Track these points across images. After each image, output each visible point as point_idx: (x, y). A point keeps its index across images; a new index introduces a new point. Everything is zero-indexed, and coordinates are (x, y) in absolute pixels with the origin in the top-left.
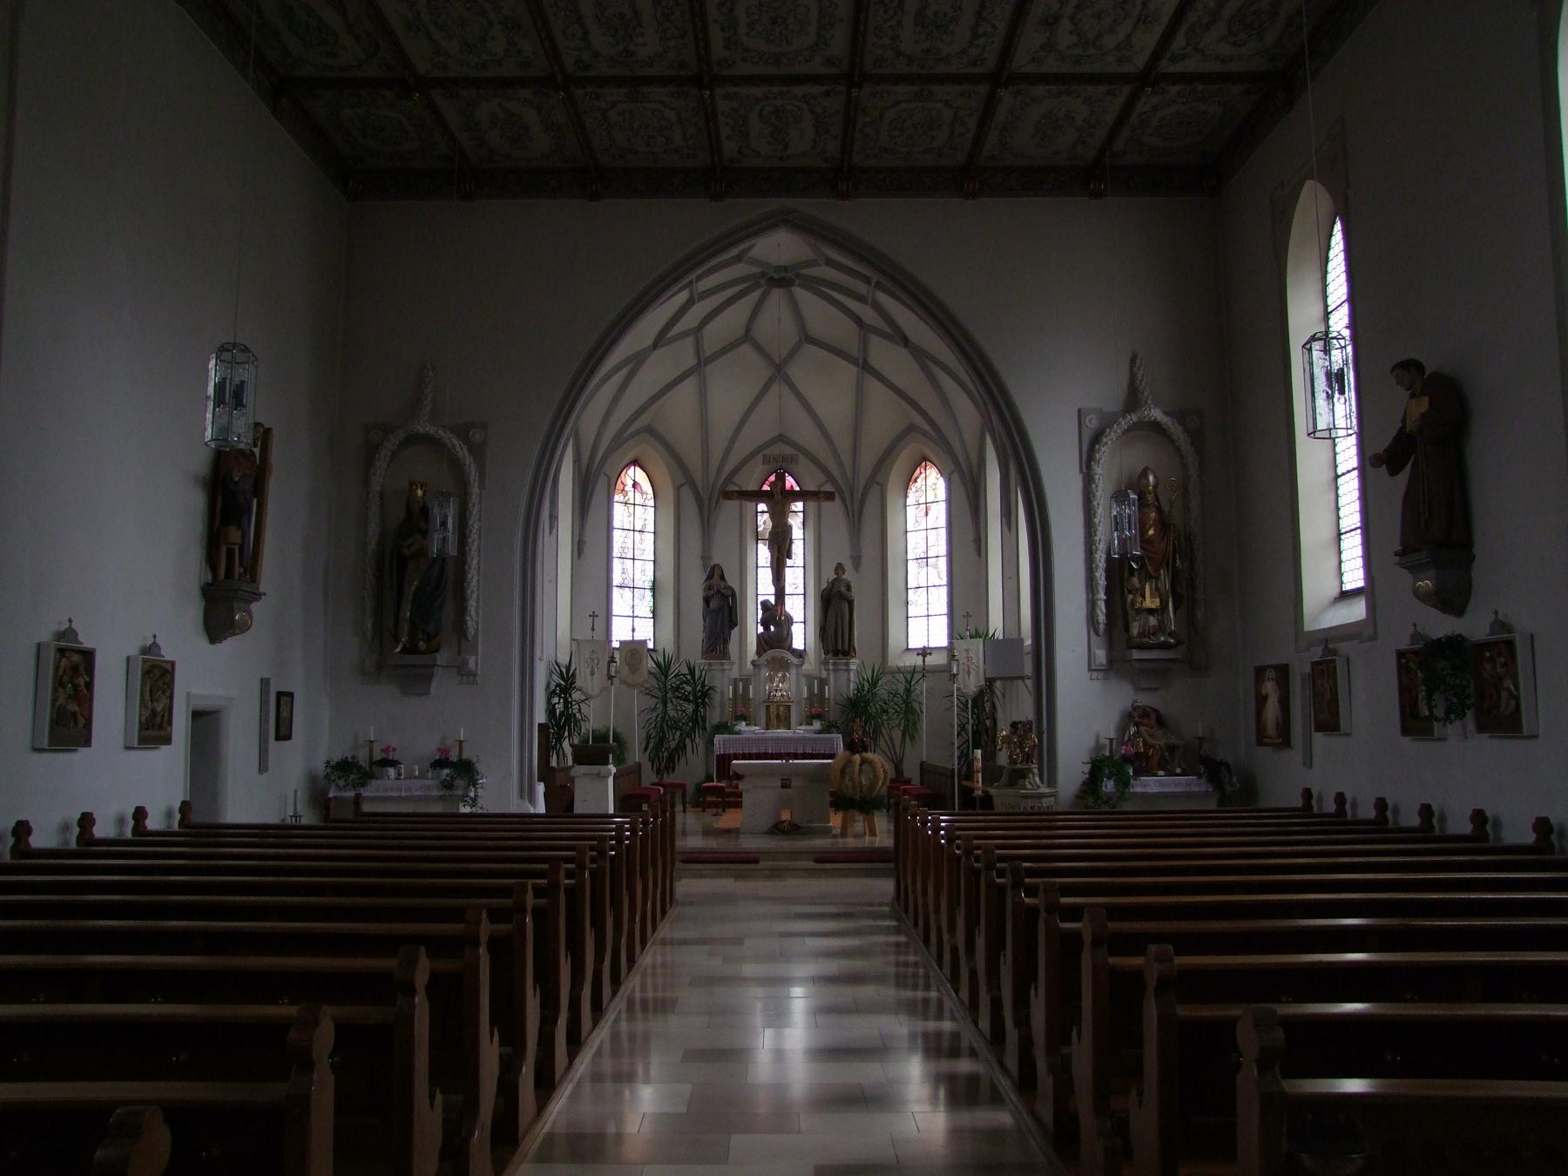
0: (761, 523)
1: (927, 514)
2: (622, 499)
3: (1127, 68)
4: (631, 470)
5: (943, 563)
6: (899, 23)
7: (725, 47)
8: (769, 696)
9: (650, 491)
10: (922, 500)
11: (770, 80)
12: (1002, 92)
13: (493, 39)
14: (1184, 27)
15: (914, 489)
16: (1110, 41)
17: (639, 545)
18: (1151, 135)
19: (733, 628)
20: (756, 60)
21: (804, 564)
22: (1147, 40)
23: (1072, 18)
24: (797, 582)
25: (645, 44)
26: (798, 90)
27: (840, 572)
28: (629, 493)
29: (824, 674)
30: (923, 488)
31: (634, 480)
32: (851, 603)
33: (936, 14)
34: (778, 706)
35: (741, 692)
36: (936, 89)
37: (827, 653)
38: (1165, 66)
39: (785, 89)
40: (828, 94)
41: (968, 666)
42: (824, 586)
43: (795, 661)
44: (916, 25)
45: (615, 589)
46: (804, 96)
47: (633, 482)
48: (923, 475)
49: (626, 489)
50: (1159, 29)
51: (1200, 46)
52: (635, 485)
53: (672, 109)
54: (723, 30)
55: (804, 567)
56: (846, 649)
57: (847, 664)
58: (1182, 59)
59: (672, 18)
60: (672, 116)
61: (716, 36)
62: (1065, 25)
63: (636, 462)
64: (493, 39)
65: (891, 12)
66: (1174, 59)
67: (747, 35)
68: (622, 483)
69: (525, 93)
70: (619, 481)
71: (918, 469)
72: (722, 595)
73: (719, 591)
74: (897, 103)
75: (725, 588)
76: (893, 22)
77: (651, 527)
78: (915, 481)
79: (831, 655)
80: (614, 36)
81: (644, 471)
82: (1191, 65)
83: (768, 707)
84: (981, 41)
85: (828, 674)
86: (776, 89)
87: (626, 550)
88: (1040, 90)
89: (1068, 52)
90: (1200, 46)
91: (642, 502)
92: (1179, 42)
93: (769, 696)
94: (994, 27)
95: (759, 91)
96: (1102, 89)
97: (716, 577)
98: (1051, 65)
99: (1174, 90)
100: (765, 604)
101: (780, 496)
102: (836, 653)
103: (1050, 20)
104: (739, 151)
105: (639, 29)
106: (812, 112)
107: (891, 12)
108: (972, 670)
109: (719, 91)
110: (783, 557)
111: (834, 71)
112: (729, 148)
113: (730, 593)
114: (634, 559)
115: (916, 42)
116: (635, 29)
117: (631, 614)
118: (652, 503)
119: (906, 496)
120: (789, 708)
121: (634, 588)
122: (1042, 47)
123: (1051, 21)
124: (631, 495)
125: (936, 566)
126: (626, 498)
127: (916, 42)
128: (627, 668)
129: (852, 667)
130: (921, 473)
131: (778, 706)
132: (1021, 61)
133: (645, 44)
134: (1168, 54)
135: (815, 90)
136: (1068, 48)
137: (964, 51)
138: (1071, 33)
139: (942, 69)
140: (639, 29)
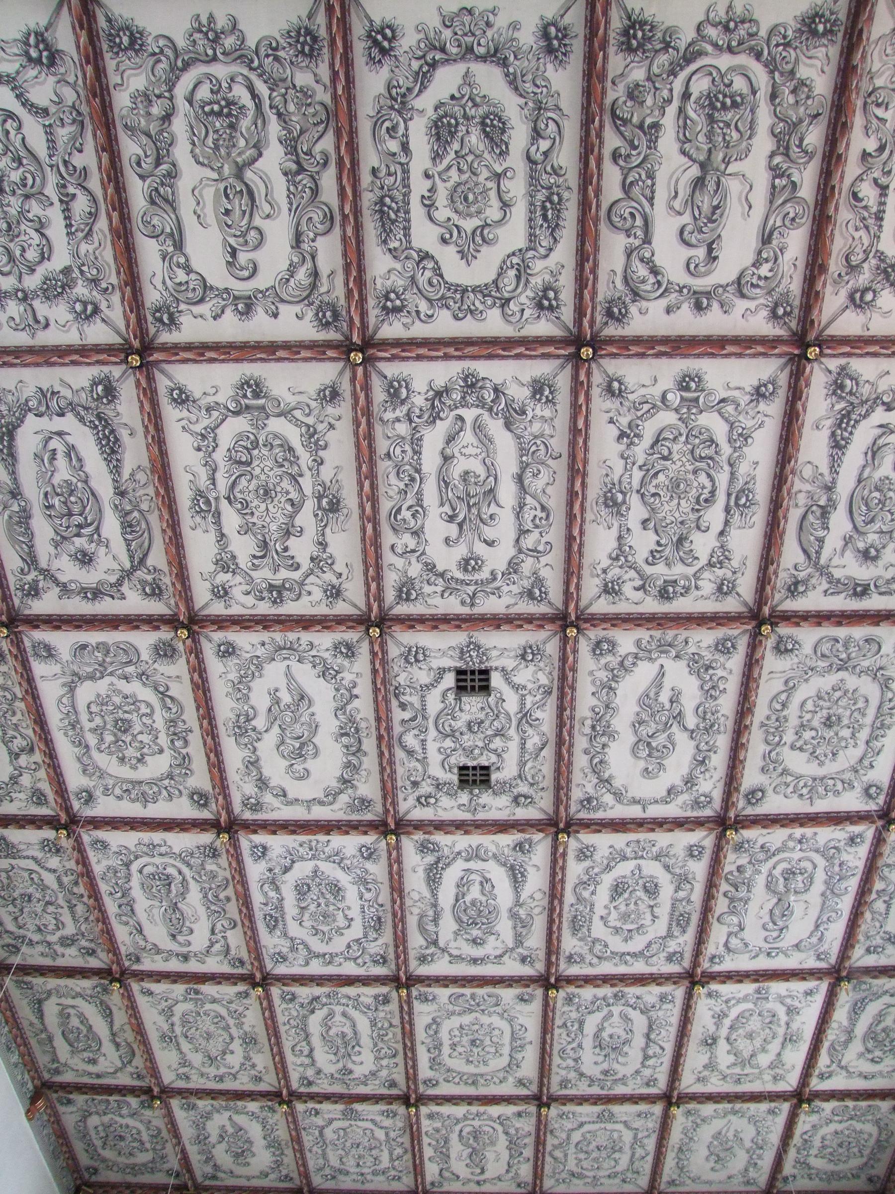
3: (782, 1087)
6: (580, 1046)
7: (431, 1068)
11: (470, 1100)
12: (674, 1110)
13: (232, 1052)
14: (826, 1045)
16: (764, 1060)
18: (816, 1156)
20: (457, 1080)
22: (796, 1057)
23: (728, 1039)
25: (362, 1063)
26: (495, 1110)
33: (611, 1036)
36: (616, 1109)
38: (816, 1084)
39: (482, 1109)
40: (519, 1114)
44: (595, 1047)
46: (499, 1118)
50: (804, 1048)
51: (843, 1063)
53: (382, 1128)
54: (429, 1051)
58: (830, 1076)
59: (386, 1038)
60: (380, 1134)
61: (423, 1058)
62: (722, 1046)
64: (232, 1052)
65: (573, 1035)
66: (822, 1076)
67: (450, 1056)
69: (253, 1106)
74: (582, 1125)
76: (574, 1045)
80: (335, 1054)
82: (838, 1082)
84: (651, 1062)
86: (474, 1109)
88: (708, 1109)
89: (729, 1072)
90: (843, 1063)
92: (823, 1060)
94: (662, 1049)
95: (459, 1111)
96: (764, 1106)
98: (715, 1085)
99: (828, 1106)
103: (709, 1041)
104: (440, 1174)
105: (357, 1048)
106: (507, 1133)
107: (573, 1035)
109: (424, 1110)
111: (524, 1092)
112: (431, 1170)
115: (596, 1063)
116: (353, 1047)
122: (705, 1067)
123: (710, 1042)
127: (596, 1063)
132: (688, 1083)
133: (362, 1063)
134: (817, 1072)
135: (509, 1110)
136: (728, 1067)
137: (637, 1072)
138: (728, 1052)
139: (620, 1090)
140: (357, 1048)
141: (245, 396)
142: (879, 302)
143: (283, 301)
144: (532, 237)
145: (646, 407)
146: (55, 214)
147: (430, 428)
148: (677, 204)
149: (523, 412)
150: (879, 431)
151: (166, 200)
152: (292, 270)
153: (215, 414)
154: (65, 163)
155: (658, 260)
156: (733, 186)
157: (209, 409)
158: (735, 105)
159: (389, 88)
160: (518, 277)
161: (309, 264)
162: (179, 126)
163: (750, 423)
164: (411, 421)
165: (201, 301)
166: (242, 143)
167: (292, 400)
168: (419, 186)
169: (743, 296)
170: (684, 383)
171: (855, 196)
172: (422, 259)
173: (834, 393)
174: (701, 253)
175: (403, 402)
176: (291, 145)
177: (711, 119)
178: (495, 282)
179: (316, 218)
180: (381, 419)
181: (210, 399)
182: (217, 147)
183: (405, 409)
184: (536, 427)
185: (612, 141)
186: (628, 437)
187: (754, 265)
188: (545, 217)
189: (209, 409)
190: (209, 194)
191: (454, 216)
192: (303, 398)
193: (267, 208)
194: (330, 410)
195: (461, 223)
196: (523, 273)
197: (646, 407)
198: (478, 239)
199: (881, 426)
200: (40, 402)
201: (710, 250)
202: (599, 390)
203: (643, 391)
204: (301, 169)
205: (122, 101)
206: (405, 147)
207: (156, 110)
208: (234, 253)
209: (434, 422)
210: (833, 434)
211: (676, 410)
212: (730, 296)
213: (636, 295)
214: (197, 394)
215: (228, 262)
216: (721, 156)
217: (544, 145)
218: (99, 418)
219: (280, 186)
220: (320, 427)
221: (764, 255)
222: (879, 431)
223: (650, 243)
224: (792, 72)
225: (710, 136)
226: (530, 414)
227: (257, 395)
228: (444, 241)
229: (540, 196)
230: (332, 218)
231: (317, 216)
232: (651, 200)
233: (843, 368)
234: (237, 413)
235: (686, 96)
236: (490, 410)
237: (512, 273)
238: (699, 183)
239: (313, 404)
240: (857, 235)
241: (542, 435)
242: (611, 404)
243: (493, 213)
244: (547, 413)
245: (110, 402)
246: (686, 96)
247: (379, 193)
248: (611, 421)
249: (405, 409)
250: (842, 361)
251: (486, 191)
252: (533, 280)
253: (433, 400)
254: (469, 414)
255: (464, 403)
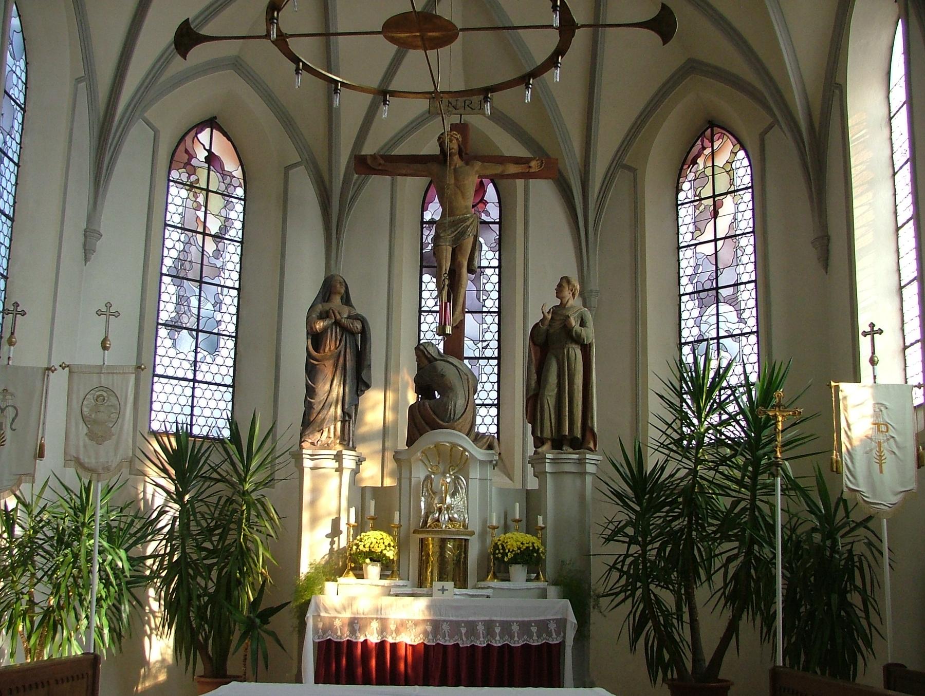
0: (429, 240)
1: (715, 215)
2: (184, 177)
4: (204, 136)
5: (747, 295)
8: (425, 522)
9: (238, 173)
10: (707, 192)
15: (691, 176)
17: (213, 261)
19: (363, 392)
21: (499, 308)
24: (488, 336)
27: (567, 293)
28: (198, 170)
29: (533, 483)
30: (709, 172)
31: (209, 151)
32: (586, 350)
34: (443, 542)
35: (372, 513)
37: (539, 442)
41: (879, 444)
42: (533, 320)
43: (478, 453)
45: (163, 332)
47: (206, 154)
48: (708, 151)
49: (194, 162)
52: (211, 159)
55: (499, 313)
56: (578, 433)
57: (581, 462)
63: (212, 123)
68: (187, 151)
70: (181, 148)
71: (699, 142)
72: (345, 329)
73: (337, 323)
75: (349, 317)
77: (235, 232)
78: (694, 162)
79: (546, 447)
81: (229, 139)
83: (423, 543)
85: (542, 484)
87: (187, 265)
91: (223, 187)
93: (425, 522)
97: (337, 301)
100: (422, 352)
101: (456, 158)
102: (558, 444)
108: (886, 454)
110: (460, 266)
113: (359, 326)
114: (201, 282)
117: (191, 377)
118: (240, 192)
119: (678, 190)
120: (463, 546)
121: (198, 331)
124: (202, 174)
125: (733, 301)
126: (193, 178)
128: (83, 429)
129: (590, 468)
130: (704, 148)
131: (443, 542)
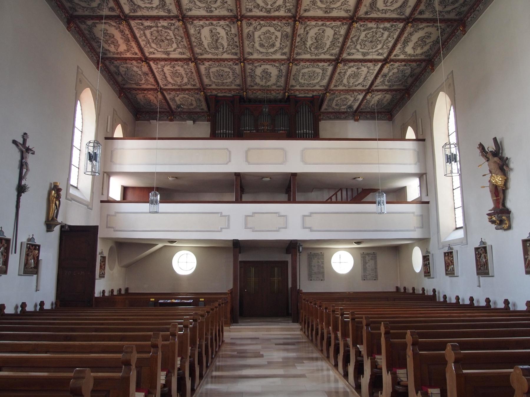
141: (330, 11)
142: (167, 24)
143: (314, 25)
144: (253, 33)
145: (221, 7)
146: (361, 38)
147: (281, 4)
148: (221, 37)
149: (254, 7)
150: (152, 3)
151: (335, 39)
152: (310, 29)
153: (340, 8)
154: (354, 44)
155: (224, 30)
156: (209, 39)
157: (341, 9)
158: (213, 48)
159: (283, 50)
160: (256, 28)
161: (306, 30)
162: (328, 46)
163: (190, 4)
164: (285, 6)
165: (334, 26)
166: (315, 45)
167: (317, 10)
168: (279, 40)
169: (201, 25)
170: (212, 11)
171: (181, 37)
172: (279, 30)
173: (169, 10)
174: (213, 31)
175: (287, 9)
176: (305, 44)
177: (217, 47)
178: (262, 27)
179: (302, 36)
180: (294, 6)
181: (340, 10)
182: (321, 45)
183: (287, 8)
184: (250, 4)
185: (238, 44)
186: (224, 2)
187: (200, 30)
188: (251, 36)
189: (341, 9)
190: (325, 39)
191: (271, 36)
192: (313, 10)
193: (313, 37)
194: (307, 8)
195: (269, 35)
196: (255, 28)
197: (221, 7)
198: (266, 33)
199: (152, 4)
200: (387, 12)
201: (212, 32)
202: (234, 10)
203: (222, 10)
204: (304, 42)
205: (338, 49)
206: (281, 44)
207: (331, 48)
208: (323, 32)
209: (279, 6)
210: (165, 2)
211: (212, 7)
212: (204, 25)
213: (228, 25)
214: (343, 11)
215: (325, 31)
216: (214, 43)
217: (252, 44)
218: (373, 9)
219: (309, 39)
220: (311, 5)
221: (199, 31)
222: (152, 3)
223: (226, 32)
224: (203, 50)
225: (217, 45)
226: (252, 6)
227: (327, 11)
228: (274, 33)
229: (252, 38)
230: (299, 36)
231: (302, 36)
232: (227, 38)
233: (170, 13)
234: (334, 8)
235: (223, 49)
236: (263, 7)
237: (258, 28)
238: (217, 40)
239: (312, 9)
240: (178, 33)
241: (249, 3)
242: (230, 8)
243: (262, 37)
244: (248, 7)
245: (368, 11)
246: (223, 49)
247: (287, 39)
248: (230, 5)
249: (287, 8)
250: (170, 15)
251: (264, 39)
252: (253, 27)
253: (279, 9)
254: (269, 7)
255: (271, 9)
